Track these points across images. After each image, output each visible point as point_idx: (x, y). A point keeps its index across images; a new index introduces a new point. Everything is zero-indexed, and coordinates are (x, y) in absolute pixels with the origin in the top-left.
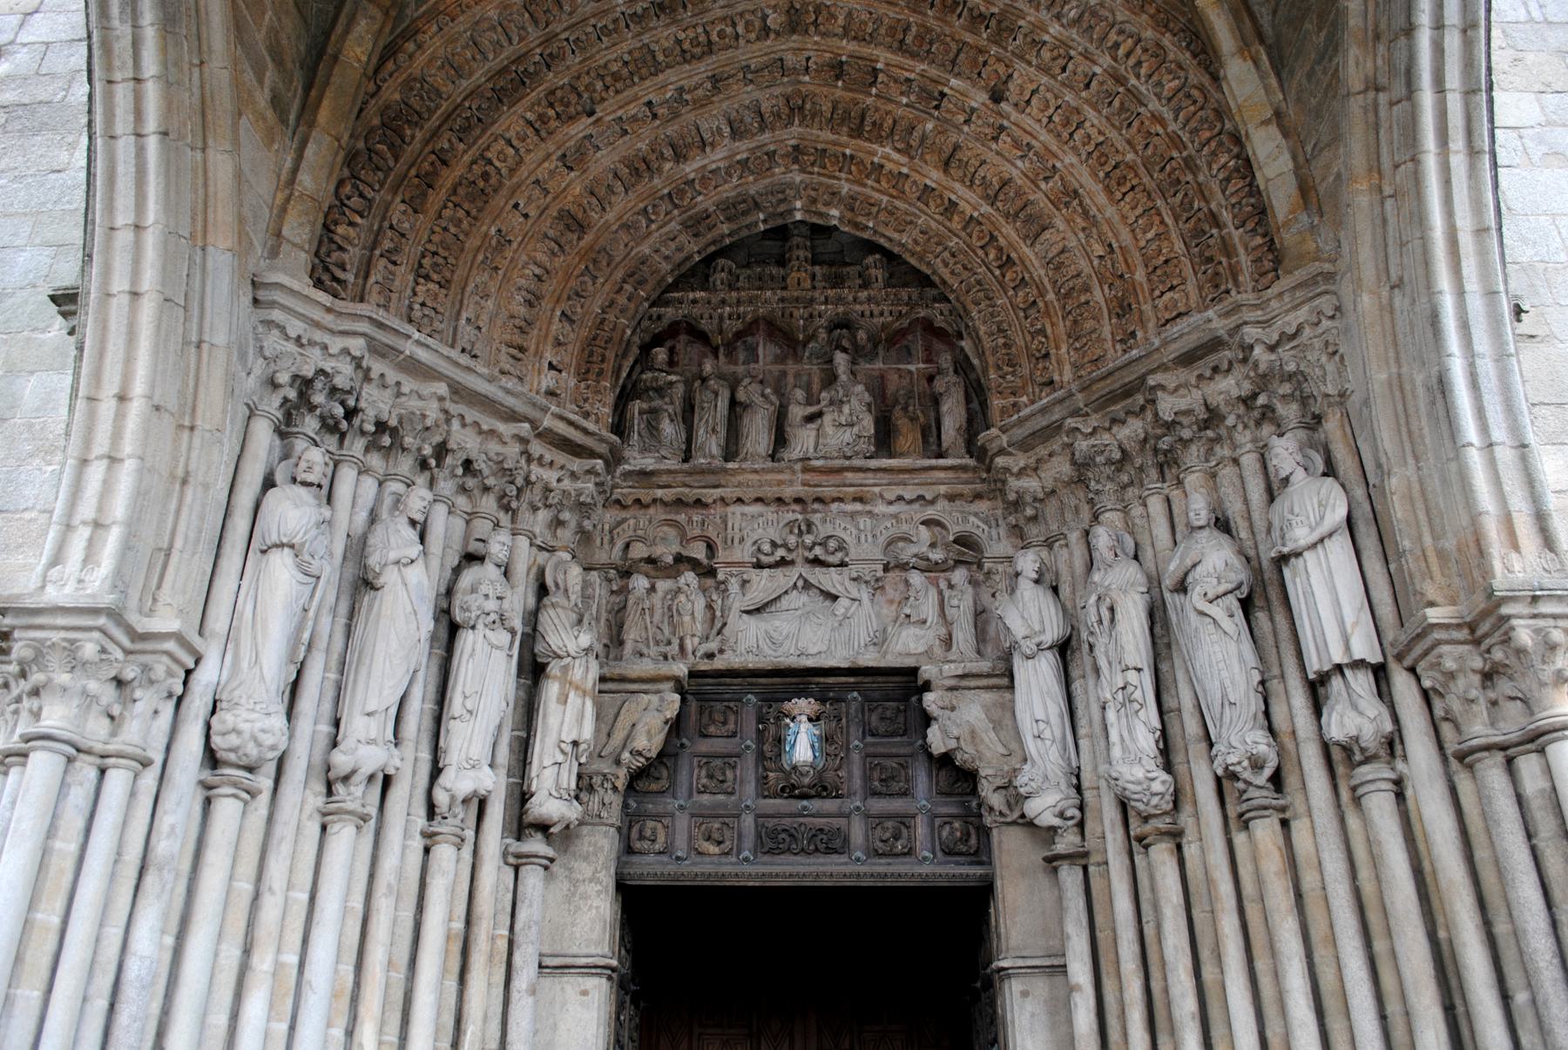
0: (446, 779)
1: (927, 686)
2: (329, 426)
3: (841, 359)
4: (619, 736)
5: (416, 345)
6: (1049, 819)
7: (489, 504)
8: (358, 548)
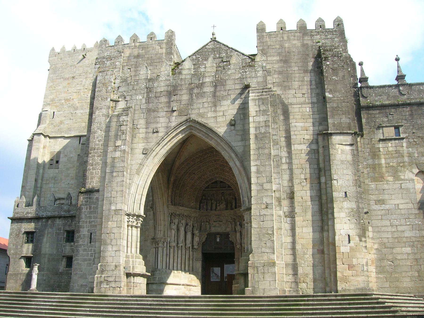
0: (187, 245)
1: (229, 234)
2: (174, 216)
3: (223, 198)
4: (201, 240)
5: (181, 208)
6: (238, 247)
7: (188, 219)
8: (178, 226)
